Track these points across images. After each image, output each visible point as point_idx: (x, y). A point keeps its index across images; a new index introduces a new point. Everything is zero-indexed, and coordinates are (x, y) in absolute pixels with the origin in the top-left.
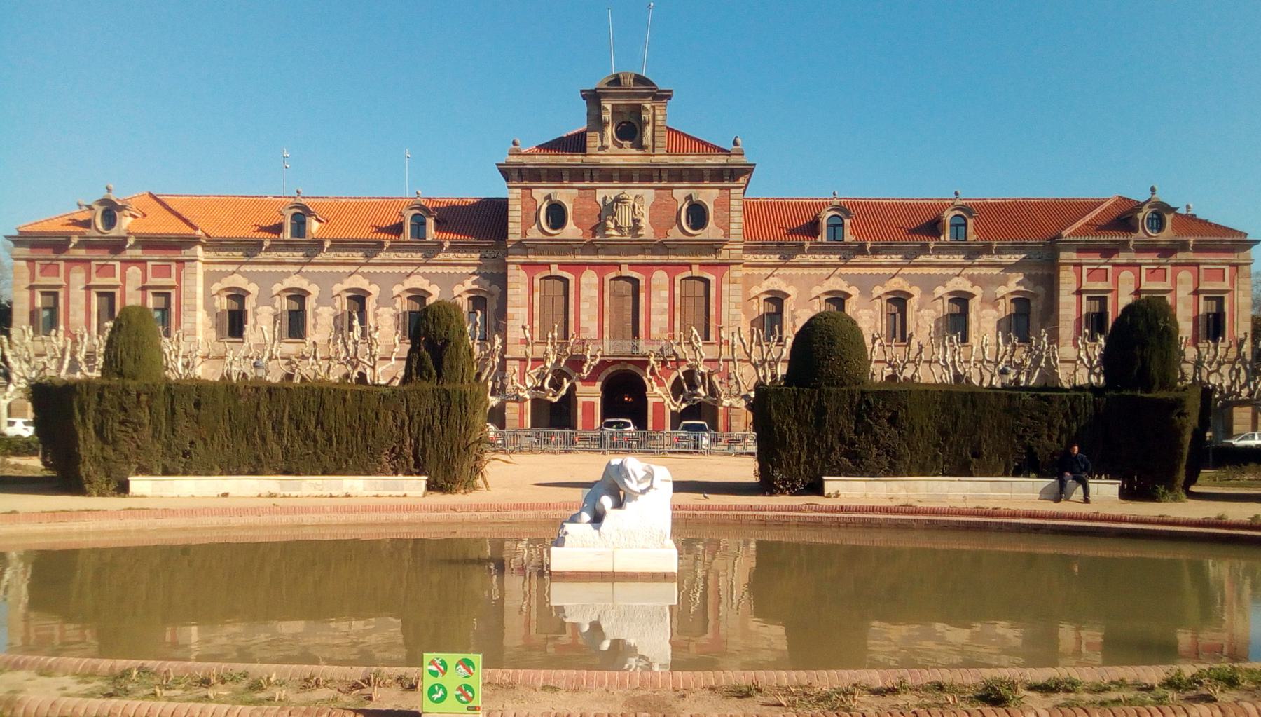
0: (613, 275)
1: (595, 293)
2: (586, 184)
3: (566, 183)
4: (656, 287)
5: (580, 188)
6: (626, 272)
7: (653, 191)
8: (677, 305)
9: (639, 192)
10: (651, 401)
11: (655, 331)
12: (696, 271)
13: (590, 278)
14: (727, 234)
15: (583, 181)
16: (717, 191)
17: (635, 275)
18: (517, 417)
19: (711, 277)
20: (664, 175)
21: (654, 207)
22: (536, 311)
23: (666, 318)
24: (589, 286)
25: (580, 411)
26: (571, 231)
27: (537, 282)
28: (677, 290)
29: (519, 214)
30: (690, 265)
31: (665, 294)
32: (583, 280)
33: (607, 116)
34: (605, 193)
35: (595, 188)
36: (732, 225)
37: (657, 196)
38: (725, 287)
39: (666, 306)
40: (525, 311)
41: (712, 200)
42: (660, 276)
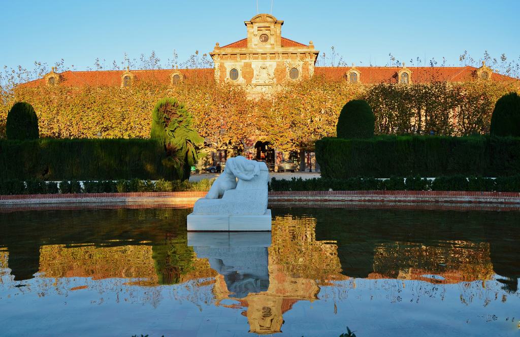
2: (247, 61)
9: (270, 63)
15: (246, 59)
21: (277, 70)
34: (256, 64)
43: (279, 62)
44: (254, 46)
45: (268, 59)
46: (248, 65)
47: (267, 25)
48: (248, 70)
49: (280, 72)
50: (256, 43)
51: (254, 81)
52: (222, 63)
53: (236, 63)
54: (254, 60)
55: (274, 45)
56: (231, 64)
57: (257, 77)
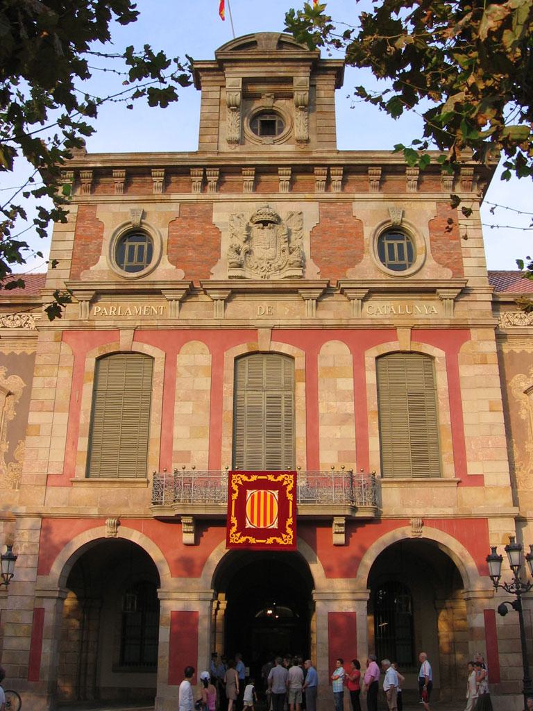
0: (242, 349)
1: (205, 383)
2: (195, 195)
3: (157, 193)
4: (330, 371)
5: (182, 204)
6: (265, 344)
7: (315, 205)
8: (372, 405)
9: (294, 207)
10: (322, 609)
11: (328, 459)
12: (403, 342)
13: (195, 356)
14: (458, 270)
16: (433, 206)
17: (285, 348)
18: (26, 643)
19: (438, 353)
20: (337, 180)
22: (84, 419)
23: (350, 431)
24: (194, 370)
25: (164, 634)
26: (164, 270)
27: (90, 363)
28: (371, 377)
29: (70, 245)
30: (388, 331)
31: (347, 384)
32: (183, 359)
33: (237, 97)
35: (211, 202)
36: (466, 262)
37: (324, 215)
38: (465, 371)
39: (350, 407)
40: (62, 419)
41: (425, 220)
42: (335, 353)
43: (330, 201)
44: (224, 147)
45: (284, 193)
46: (199, 215)
47: (282, 71)
48: (198, 233)
49: (335, 237)
50: (236, 135)
51: (221, 273)
52: (88, 204)
53: (148, 207)
54: (223, 196)
55: (308, 141)
56: (126, 208)
57: (236, 259)
